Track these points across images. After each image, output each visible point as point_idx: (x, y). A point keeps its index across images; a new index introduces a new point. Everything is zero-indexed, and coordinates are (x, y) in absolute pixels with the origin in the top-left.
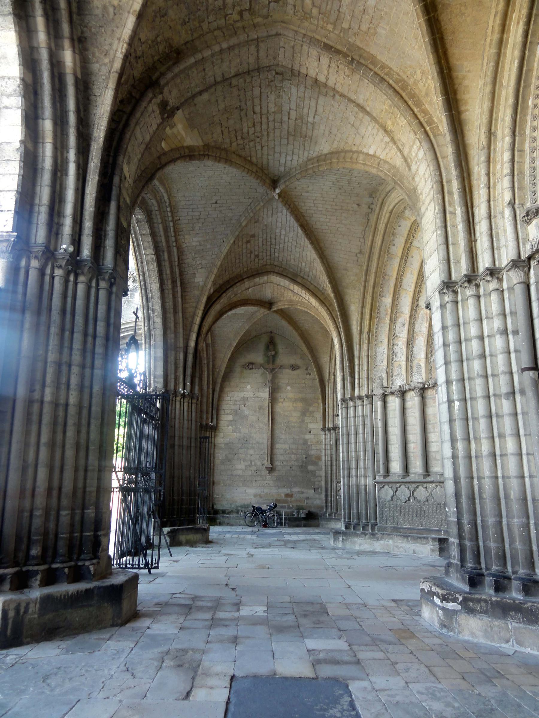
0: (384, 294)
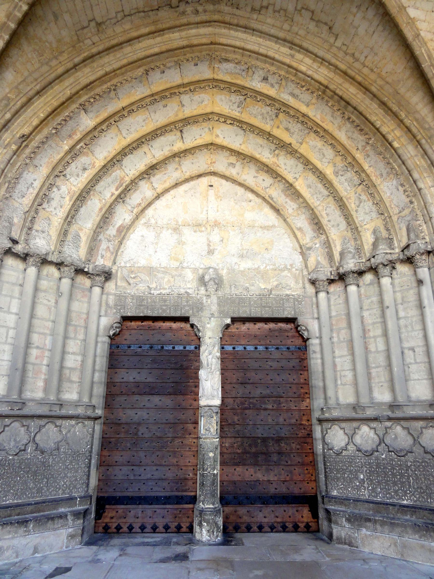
0: (90, 108)
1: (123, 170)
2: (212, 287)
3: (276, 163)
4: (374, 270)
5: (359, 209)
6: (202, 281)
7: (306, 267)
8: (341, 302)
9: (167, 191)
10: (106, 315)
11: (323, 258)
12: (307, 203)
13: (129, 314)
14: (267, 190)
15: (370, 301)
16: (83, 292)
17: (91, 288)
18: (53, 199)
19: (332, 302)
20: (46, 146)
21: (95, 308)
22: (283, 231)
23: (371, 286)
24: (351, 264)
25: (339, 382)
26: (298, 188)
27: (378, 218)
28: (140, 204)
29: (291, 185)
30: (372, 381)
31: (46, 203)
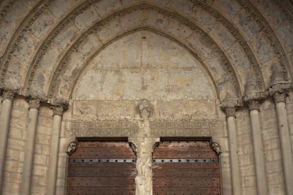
1: (76, 26)
2: (145, 114)
3: (194, 17)
4: (272, 98)
5: (260, 50)
6: (138, 110)
7: (219, 98)
8: (246, 124)
9: (110, 42)
10: (65, 137)
11: (231, 91)
12: (219, 48)
13: (82, 136)
14: (188, 39)
15: (268, 122)
16: (47, 119)
17: (53, 116)
18: (22, 48)
19: (239, 125)
20: (14, 6)
21: (57, 131)
22: (200, 71)
23: (269, 111)
24: (253, 94)
25: (244, 185)
26: (212, 36)
27: (275, 57)
28: (89, 53)
29: (206, 35)
30: (269, 183)
31: (16, 51)
